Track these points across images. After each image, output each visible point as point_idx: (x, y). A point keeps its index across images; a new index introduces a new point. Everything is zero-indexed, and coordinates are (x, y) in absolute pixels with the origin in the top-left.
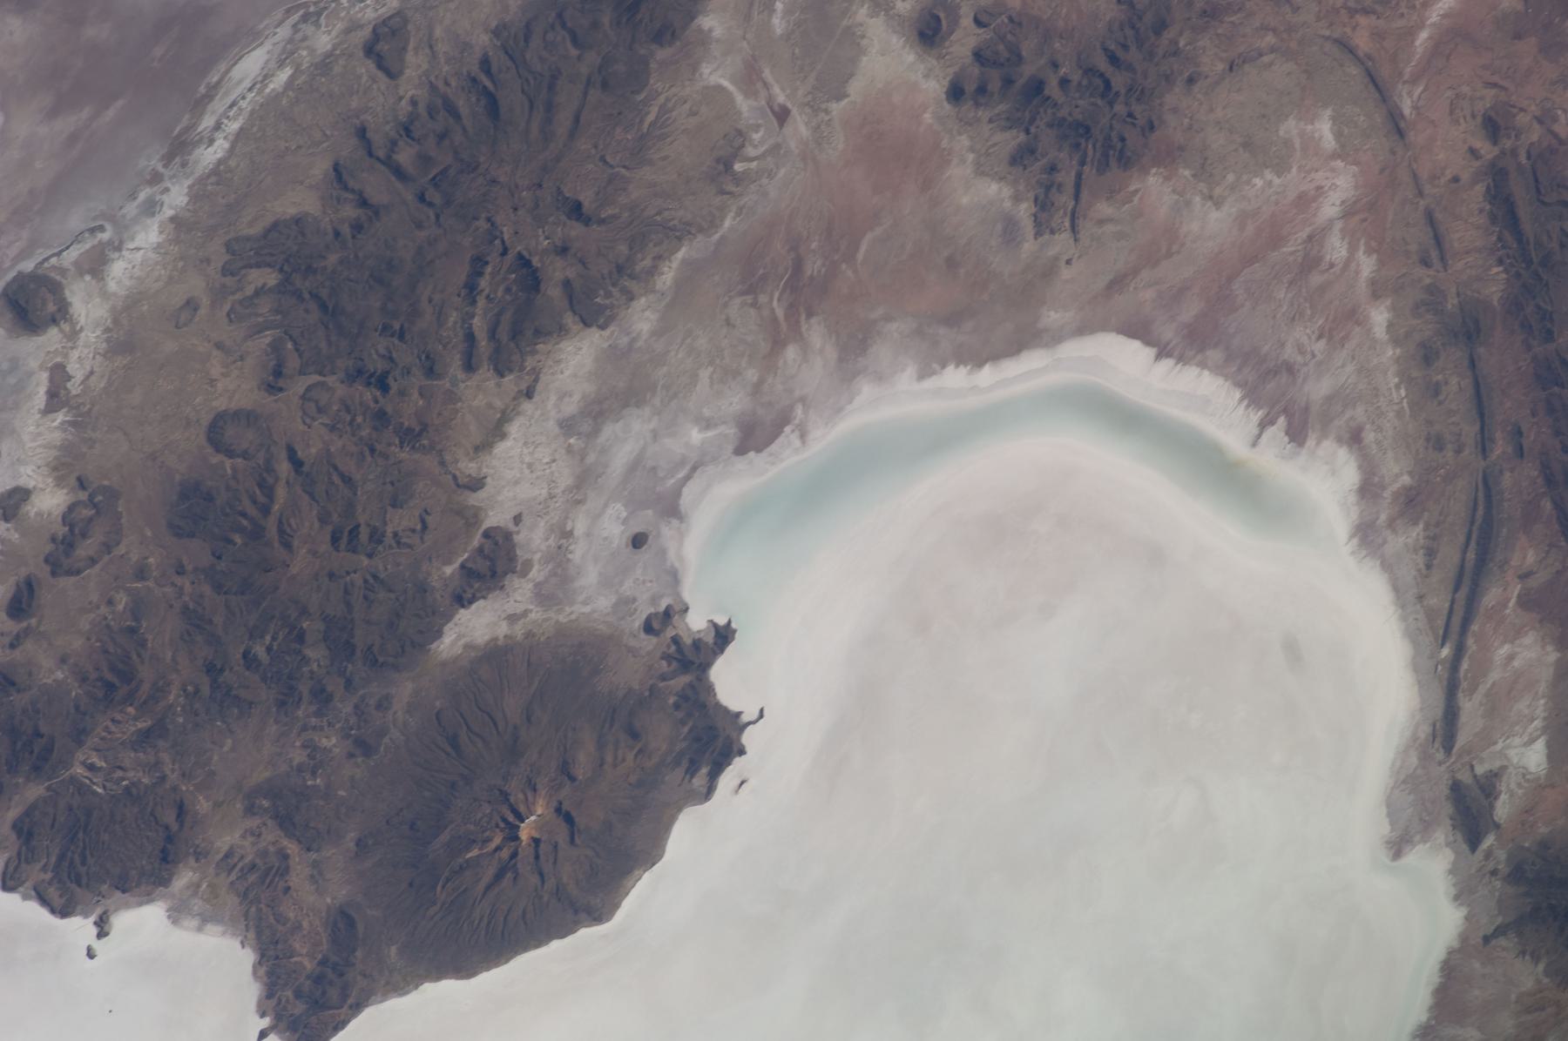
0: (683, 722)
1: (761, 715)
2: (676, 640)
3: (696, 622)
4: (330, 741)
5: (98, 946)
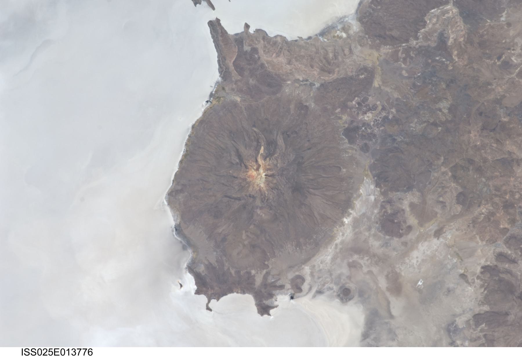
0: (238, 272)
2: (282, 287)
3: (282, 300)
4: (369, 117)
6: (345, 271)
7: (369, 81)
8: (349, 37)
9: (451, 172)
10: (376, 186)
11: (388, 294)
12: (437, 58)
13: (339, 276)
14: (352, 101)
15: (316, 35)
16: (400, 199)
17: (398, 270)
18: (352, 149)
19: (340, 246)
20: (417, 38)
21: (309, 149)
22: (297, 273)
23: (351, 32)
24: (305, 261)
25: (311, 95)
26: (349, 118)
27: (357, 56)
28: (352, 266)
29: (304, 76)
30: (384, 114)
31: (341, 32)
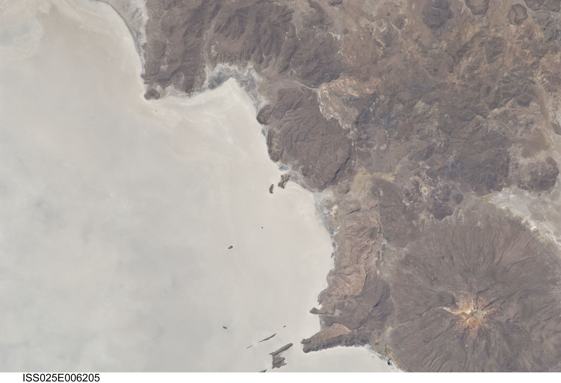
4: (425, 190)
5: (276, 189)
7: (387, 186)
8: (338, 203)
9: (494, 108)
10: (500, 191)
12: (371, 110)
14: (406, 207)
15: (332, 237)
16: (517, 167)
18: (458, 212)
20: (348, 131)
21: (452, 258)
23: (333, 199)
25: (395, 249)
26: (424, 212)
27: (359, 196)
29: (374, 255)
30: (424, 174)
31: (332, 210)
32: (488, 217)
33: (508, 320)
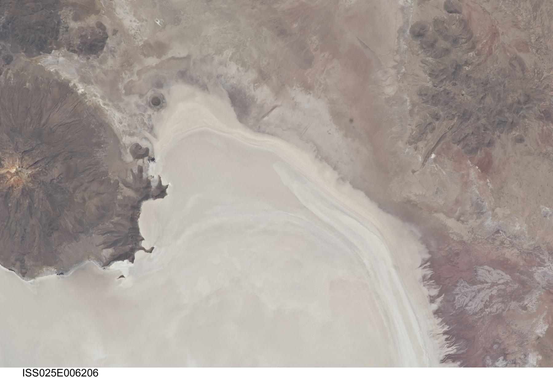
1: (151, 251)
2: (141, 170)
3: (153, 171)
6: (134, 99)
10: (50, 53)
11: (164, 58)
13: (138, 106)
17: (141, 43)
19: (107, 101)
22: (128, 150)
24: (117, 140)
28: (129, 91)
32: (37, 79)
33: (51, 180)
